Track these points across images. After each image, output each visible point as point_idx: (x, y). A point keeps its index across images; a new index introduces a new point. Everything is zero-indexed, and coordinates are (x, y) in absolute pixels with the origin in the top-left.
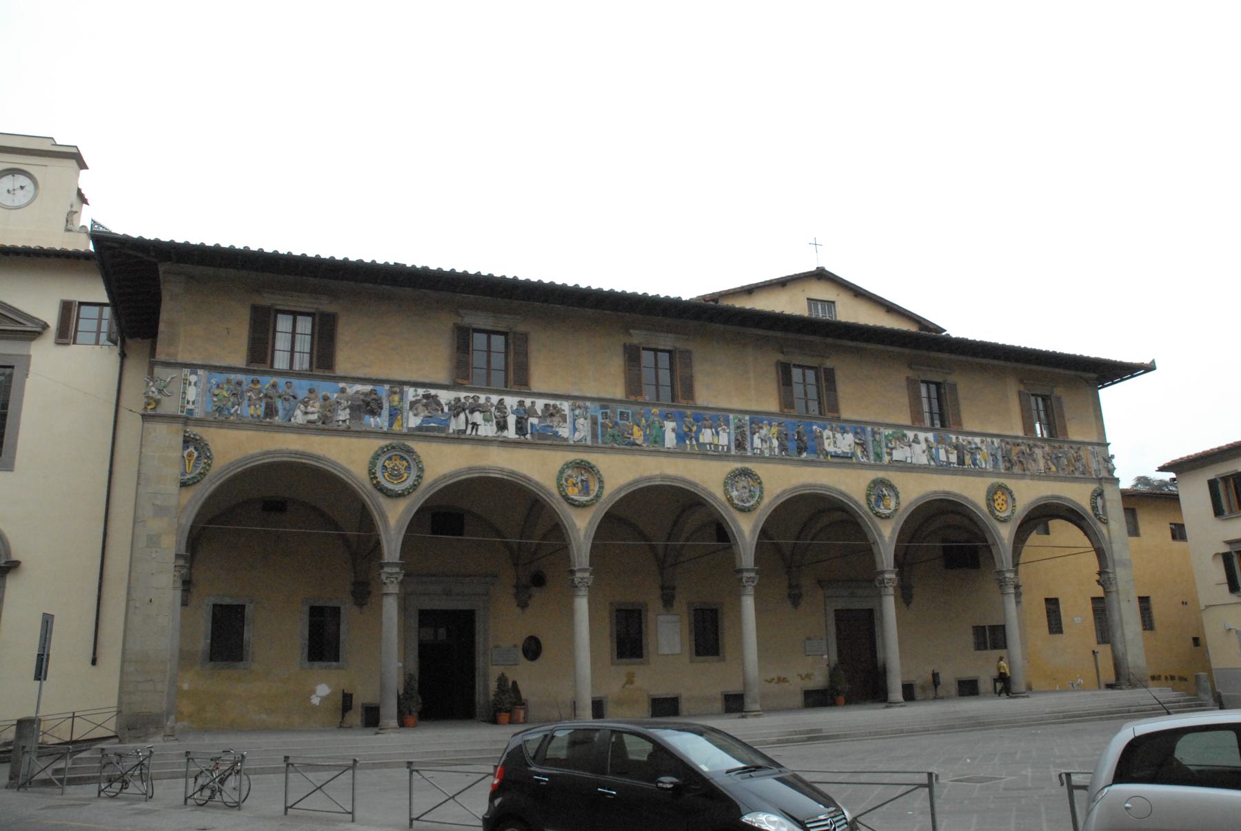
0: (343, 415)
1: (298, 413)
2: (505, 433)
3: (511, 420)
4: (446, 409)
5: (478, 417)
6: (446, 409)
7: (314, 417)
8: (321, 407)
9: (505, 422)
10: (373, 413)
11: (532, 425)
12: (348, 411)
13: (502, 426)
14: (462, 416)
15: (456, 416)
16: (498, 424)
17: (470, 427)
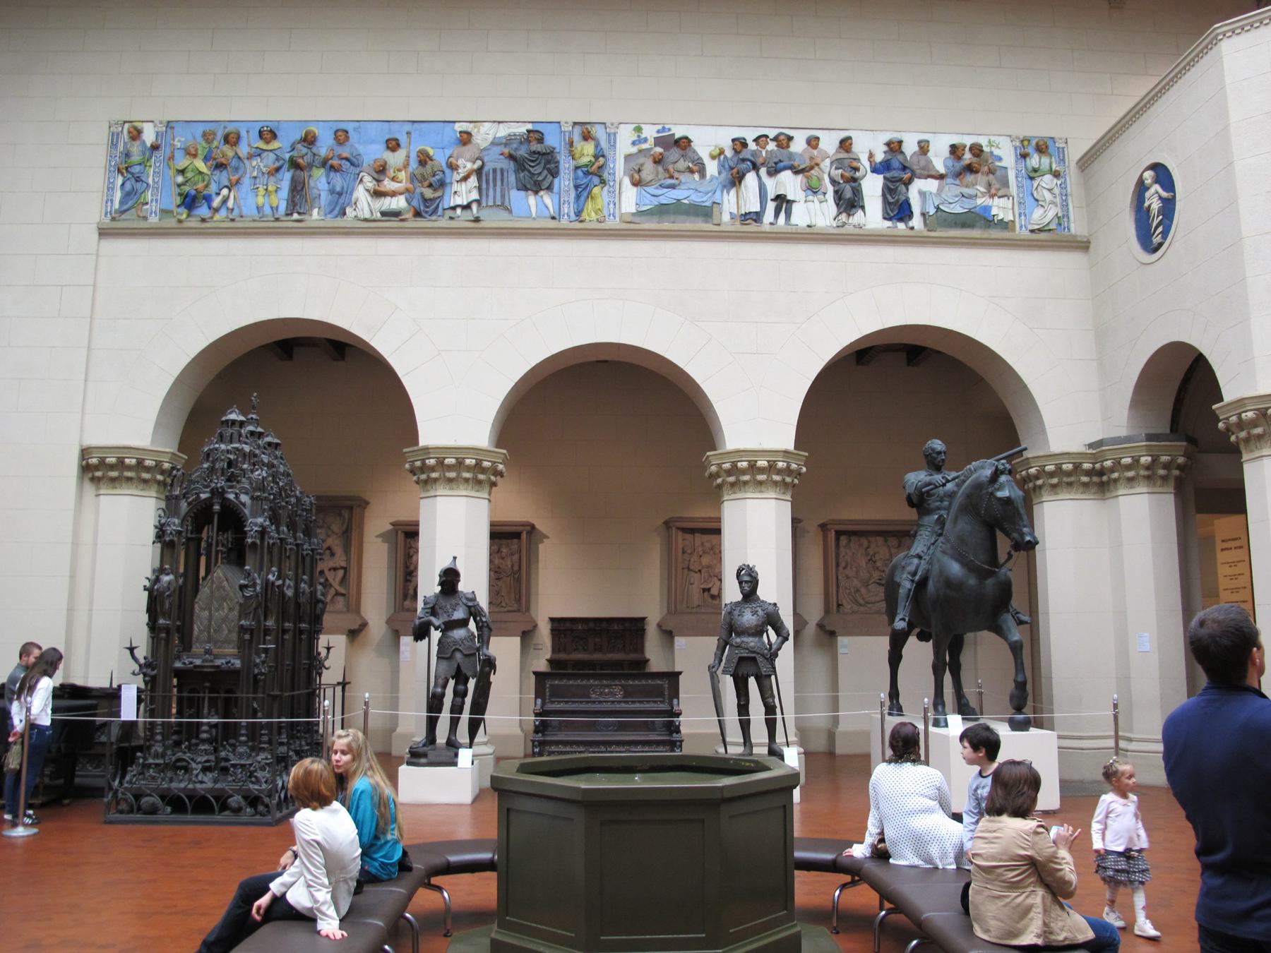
0: (464, 192)
1: (361, 194)
2: (858, 217)
3: (872, 187)
4: (712, 168)
5: (789, 183)
6: (712, 168)
7: (399, 203)
8: (413, 178)
9: (857, 192)
10: (536, 187)
11: (922, 194)
12: (473, 181)
13: (849, 202)
14: (751, 178)
15: (736, 180)
16: (838, 196)
17: (771, 207)
